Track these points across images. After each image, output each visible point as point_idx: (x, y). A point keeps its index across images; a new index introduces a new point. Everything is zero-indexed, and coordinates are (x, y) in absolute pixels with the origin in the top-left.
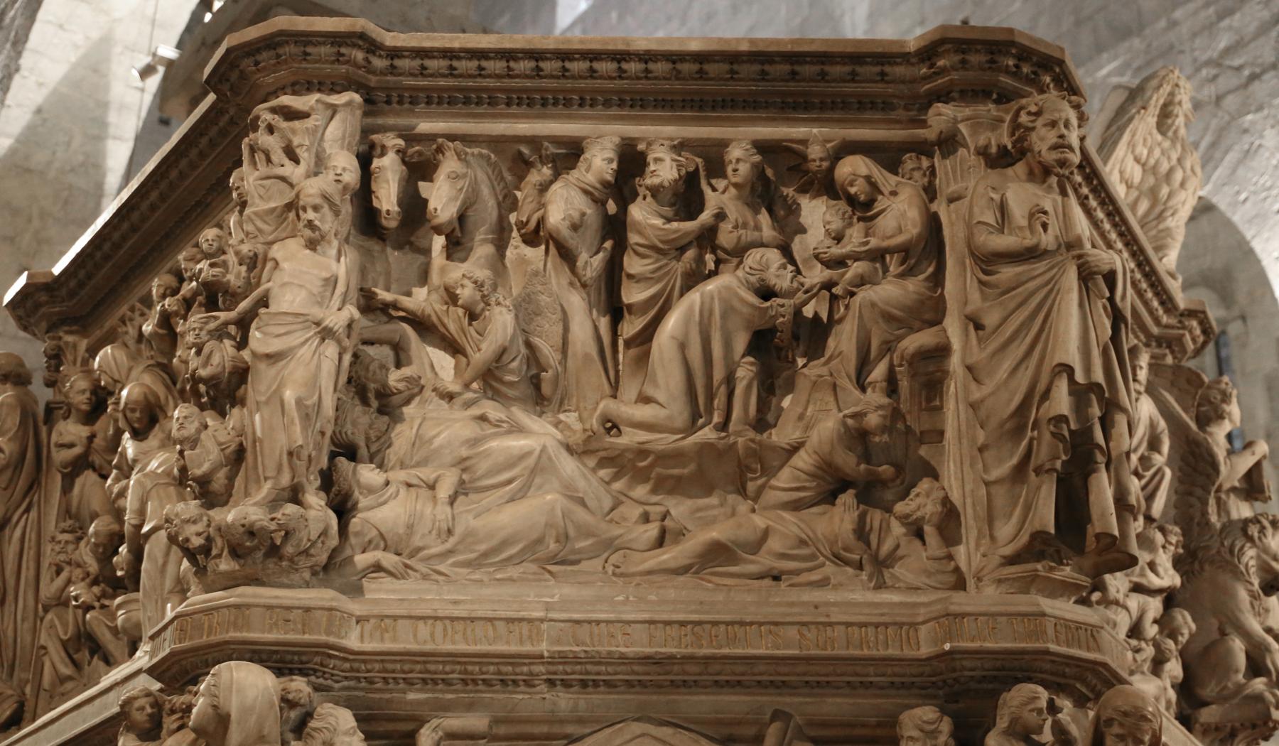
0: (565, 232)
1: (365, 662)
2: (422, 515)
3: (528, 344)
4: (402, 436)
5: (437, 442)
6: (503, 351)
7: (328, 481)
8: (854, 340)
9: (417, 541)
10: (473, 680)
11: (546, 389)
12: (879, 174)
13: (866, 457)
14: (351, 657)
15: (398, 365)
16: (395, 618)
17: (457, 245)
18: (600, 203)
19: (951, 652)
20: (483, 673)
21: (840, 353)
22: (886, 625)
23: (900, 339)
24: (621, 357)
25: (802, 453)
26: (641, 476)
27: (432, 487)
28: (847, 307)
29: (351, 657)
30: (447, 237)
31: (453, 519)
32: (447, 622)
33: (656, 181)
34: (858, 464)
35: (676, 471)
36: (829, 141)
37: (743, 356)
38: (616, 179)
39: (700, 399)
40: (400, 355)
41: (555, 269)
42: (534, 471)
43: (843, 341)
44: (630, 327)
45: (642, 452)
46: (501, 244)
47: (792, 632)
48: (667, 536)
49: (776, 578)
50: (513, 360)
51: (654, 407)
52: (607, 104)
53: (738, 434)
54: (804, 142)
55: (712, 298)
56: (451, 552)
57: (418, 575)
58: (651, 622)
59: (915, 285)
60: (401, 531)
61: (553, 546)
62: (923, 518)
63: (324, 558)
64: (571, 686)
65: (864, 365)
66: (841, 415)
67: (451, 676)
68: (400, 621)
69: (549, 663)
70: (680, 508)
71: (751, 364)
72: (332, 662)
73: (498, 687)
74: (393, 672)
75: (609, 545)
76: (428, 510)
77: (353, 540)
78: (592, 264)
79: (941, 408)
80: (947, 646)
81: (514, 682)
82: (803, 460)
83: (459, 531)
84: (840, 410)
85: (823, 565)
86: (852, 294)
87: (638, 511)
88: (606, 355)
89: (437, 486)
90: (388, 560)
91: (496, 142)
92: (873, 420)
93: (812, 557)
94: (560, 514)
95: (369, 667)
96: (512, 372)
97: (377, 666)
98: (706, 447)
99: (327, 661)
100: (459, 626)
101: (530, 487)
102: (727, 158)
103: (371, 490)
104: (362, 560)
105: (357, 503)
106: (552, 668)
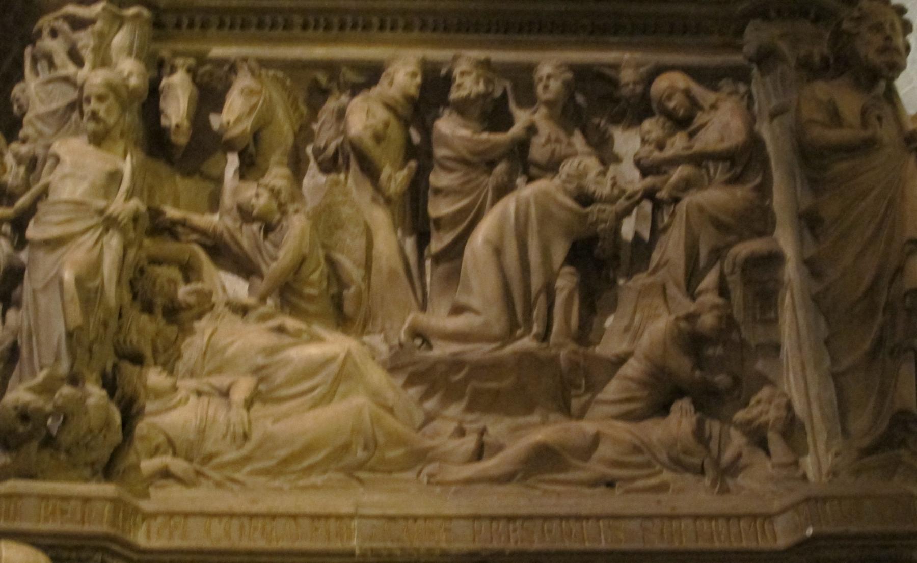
0: (368, 142)
2: (214, 421)
3: (331, 262)
4: (192, 348)
5: (231, 351)
6: (302, 261)
7: (110, 384)
8: (682, 246)
9: (209, 447)
11: (349, 307)
12: (697, 90)
13: (699, 362)
15: (187, 280)
16: (187, 515)
17: (250, 167)
18: (406, 124)
19: (814, 538)
21: (667, 262)
22: (739, 517)
23: (729, 246)
24: (428, 279)
25: (632, 361)
26: (451, 394)
27: (225, 394)
28: (673, 215)
30: (241, 155)
31: (250, 422)
32: (246, 521)
33: (463, 93)
34: (693, 370)
35: (493, 385)
36: (643, 65)
37: (562, 266)
38: (421, 94)
39: (520, 304)
40: (189, 271)
41: (357, 184)
42: (338, 379)
43: (672, 248)
44: (437, 244)
45: (456, 364)
46: (297, 167)
47: (634, 525)
48: (486, 448)
49: (610, 484)
50: (314, 271)
51: (468, 312)
52: (408, 27)
53: (560, 346)
54: (616, 67)
55: (528, 205)
56: (247, 459)
57: (211, 483)
58: (476, 517)
59: (742, 193)
60: (192, 436)
61: (360, 454)
62: (767, 423)
63: (106, 453)
65: (693, 276)
66: (673, 317)
68: (192, 521)
70: (497, 427)
71: (571, 274)
75: (420, 457)
76: (221, 417)
77: (138, 445)
78: (396, 178)
79: (776, 321)
80: (810, 532)
82: (632, 368)
83: (255, 436)
84: (670, 314)
85: (660, 472)
86: (676, 200)
87: (453, 426)
88: (413, 276)
89: (231, 392)
90: (178, 465)
91: (293, 67)
92: (708, 320)
93: (648, 465)
94: (367, 419)
96: (311, 285)
98: (524, 356)
100: (259, 523)
101: (333, 396)
102: (536, 77)
103: (158, 394)
104: (148, 465)
105: (143, 407)
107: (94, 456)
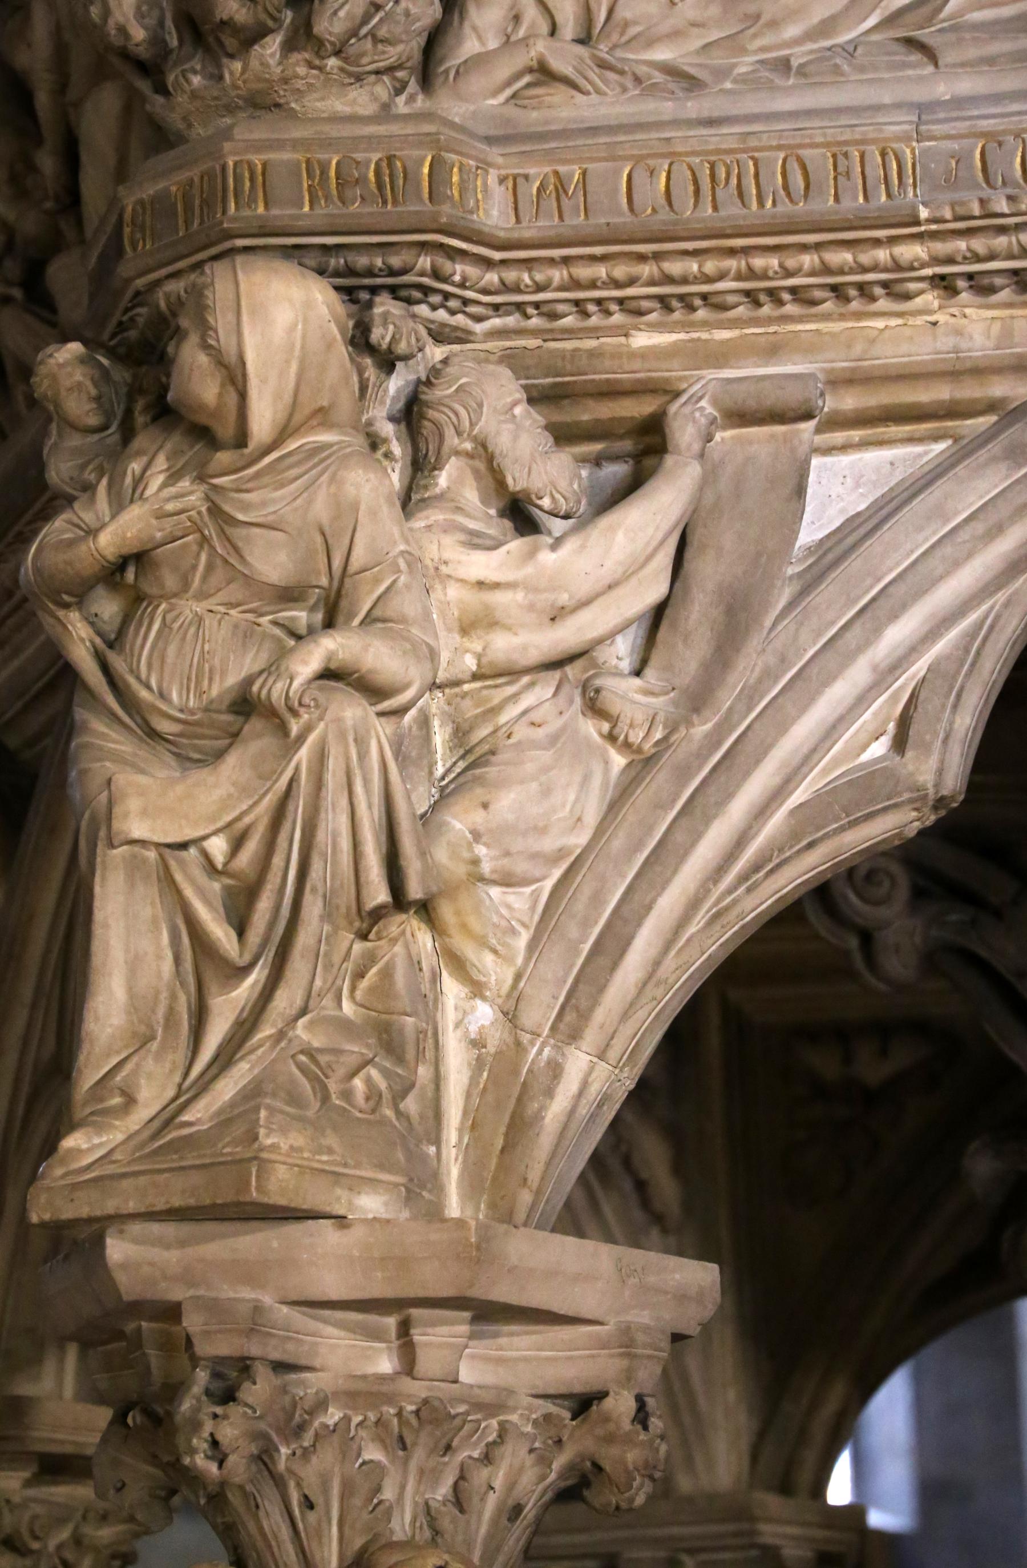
1: (527, 263)
10: (771, 293)
14: (497, 256)
20: (789, 274)
29: (497, 256)
63: (412, 47)
64: (992, 290)
67: (721, 286)
69: (934, 235)
72: (459, 270)
73: (828, 306)
74: (593, 285)
81: (863, 288)
95: (539, 277)
97: (558, 275)
99: (447, 266)
106: (942, 248)
107: (393, 54)
